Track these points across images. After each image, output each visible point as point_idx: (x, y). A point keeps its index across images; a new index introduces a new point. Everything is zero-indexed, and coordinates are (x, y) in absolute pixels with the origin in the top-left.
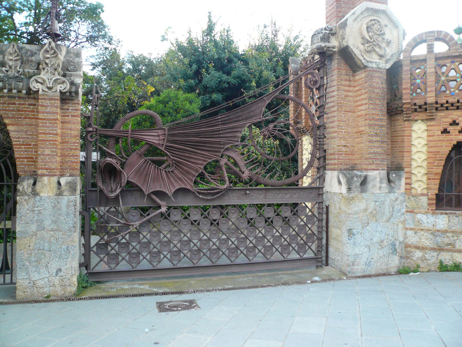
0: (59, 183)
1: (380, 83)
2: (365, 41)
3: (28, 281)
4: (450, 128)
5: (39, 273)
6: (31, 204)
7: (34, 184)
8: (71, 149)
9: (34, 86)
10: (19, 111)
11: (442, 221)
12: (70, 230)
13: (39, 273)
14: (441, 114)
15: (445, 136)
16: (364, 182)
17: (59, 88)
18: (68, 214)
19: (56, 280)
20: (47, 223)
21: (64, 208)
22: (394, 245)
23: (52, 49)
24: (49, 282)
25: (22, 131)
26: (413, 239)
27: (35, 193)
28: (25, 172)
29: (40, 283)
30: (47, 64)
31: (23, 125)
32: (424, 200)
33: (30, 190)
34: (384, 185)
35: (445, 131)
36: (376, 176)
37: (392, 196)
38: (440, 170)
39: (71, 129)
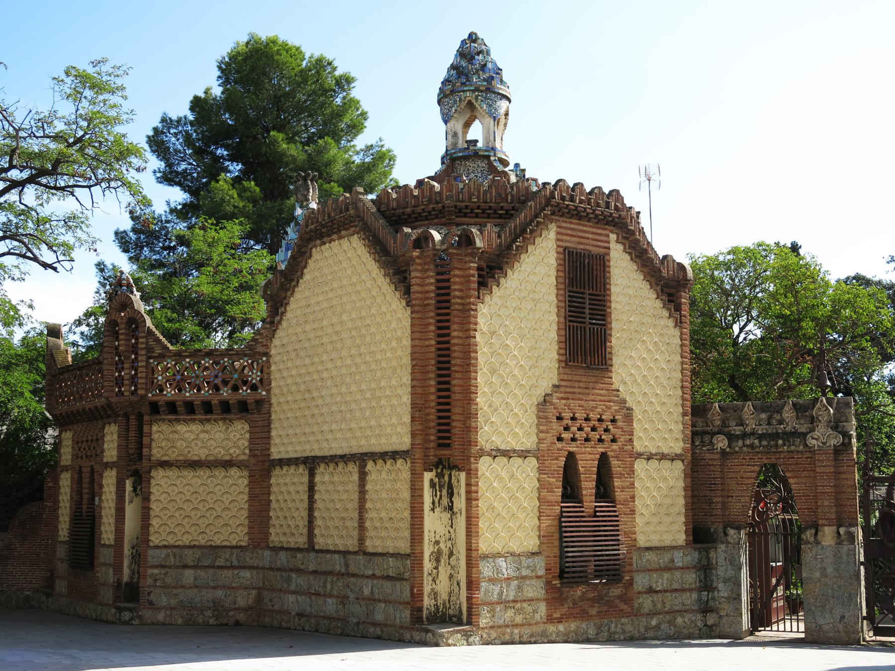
0: (838, 533)
3: (814, 625)
5: (825, 618)
6: (814, 552)
7: (816, 534)
8: (848, 499)
9: (811, 442)
10: (797, 464)
12: (851, 578)
13: (825, 618)
17: (833, 442)
18: (848, 563)
19: (840, 627)
20: (829, 570)
21: (845, 557)
23: (824, 406)
24: (834, 627)
25: (802, 483)
27: (818, 543)
28: (806, 522)
29: (826, 628)
30: (820, 421)
31: (801, 478)
33: (813, 539)
39: (847, 479)
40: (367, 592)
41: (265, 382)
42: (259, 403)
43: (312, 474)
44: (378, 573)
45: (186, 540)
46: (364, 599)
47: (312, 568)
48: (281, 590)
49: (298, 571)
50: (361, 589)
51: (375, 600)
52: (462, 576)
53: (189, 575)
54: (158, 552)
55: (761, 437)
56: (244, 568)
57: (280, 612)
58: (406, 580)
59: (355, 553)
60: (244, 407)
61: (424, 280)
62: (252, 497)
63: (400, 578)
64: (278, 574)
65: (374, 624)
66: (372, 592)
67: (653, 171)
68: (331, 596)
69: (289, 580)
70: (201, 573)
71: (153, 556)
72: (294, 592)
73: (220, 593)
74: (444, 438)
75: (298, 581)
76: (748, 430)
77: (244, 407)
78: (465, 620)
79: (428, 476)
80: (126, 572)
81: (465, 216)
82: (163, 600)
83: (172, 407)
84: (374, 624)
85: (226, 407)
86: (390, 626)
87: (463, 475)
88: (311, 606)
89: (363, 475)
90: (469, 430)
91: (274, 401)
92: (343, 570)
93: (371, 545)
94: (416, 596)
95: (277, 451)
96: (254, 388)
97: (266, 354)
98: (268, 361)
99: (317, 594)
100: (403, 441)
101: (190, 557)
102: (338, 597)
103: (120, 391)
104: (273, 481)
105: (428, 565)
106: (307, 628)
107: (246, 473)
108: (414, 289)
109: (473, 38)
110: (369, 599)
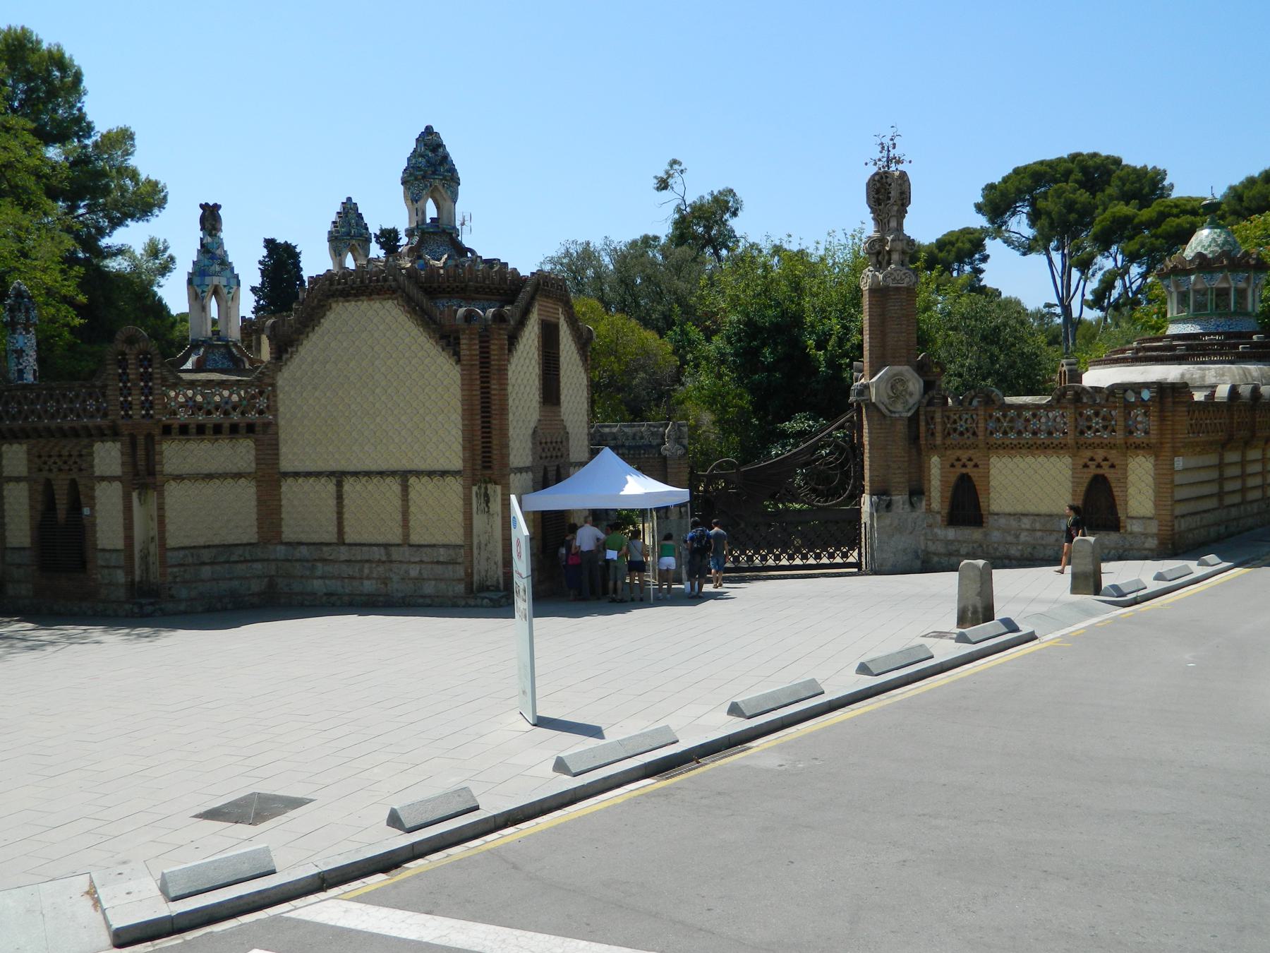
1: (901, 428)
2: (890, 398)
4: (956, 463)
11: (951, 533)
14: (949, 452)
15: (952, 470)
16: (889, 506)
22: (916, 552)
26: (932, 547)
27: (667, 518)
32: (939, 518)
34: (907, 506)
35: (953, 466)
36: (899, 499)
37: (914, 515)
38: (949, 494)
40: (414, 571)
41: (272, 408)
42: (267, 425)
43: (339, 485)
44: (425, 559)
45: (201, 541)
47: (343, 558)
49: (324, 561)
50: (407, 572)
52: (499, 557)
53: (206, 571)
54: (176, 553)
55: (630, 448)
56: (257, 561)
59: (398, 545)
60: (251, 428)
61: (469, 346)
62: (261, 502)
63: (453, 562)
64: (298, 565)
67: (467, 218)
68: (368, 578)
70: (218, 568)
71: (173, 557)
72: (321, 578)
73: (236, 583)
74: (487, 463)
75: (320, 569)
76: (619, 443)
77: (251, 428)
78: (502, 586)
79: (475, 489)
80: (137, 572)
81: (478, 293)
82: (184, 593)
83: (184, 430)
84: (422, 597)
85: (234, 429)
87: (499, 488)
89: (405, 489)
90: (505, 456)
91: (282, 422)
92: (384, 558)
93: (415, 538)
94: (470, 575)
95: (286, 465)
96: (261, 412)
97: (273, 385)
98: (274, 391)
100: (457, 464)
101: (206, 555)
103: (127, 414)
104: (284, 489)
105: (475, 551)
107: (253, 483)
108: (462, 353)
109: (429, 130)
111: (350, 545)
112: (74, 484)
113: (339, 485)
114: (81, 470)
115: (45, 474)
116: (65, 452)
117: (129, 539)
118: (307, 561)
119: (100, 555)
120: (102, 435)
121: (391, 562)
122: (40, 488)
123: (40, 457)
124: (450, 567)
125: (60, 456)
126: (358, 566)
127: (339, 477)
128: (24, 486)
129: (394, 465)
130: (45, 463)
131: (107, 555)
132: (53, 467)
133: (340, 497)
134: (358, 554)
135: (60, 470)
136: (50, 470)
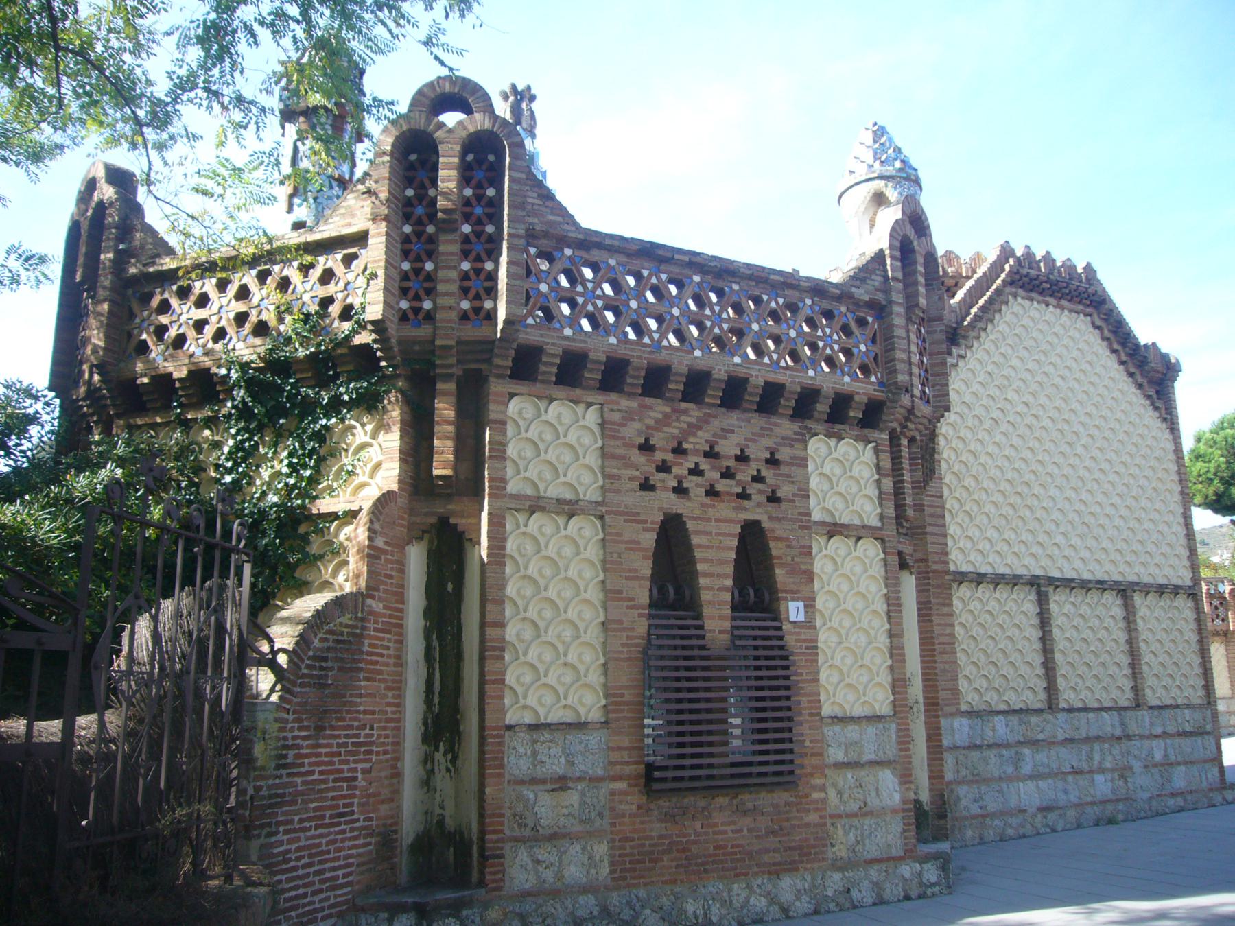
40: (1158, 756)
44: (1171, 729)
46: (1155, 766)
47: (1061, 736)
48: (1000, 778)
49: (1034, 743)
50: (1150, 753)
51: (1171, 764)
57: (1001, 814)
58: (1208, 733)
64: (992, 754)
65: (1173, 795)
66: (1166, 755)
68: (1102, 771)
69: (1017, 760)
84: (1173, 795)
86: (1196, 791)
88: (1066, 792)
92: (1118, 732)
99: (1076, 772)
102: (1113, 770)
106: (1059, 827)
110: (1163, 765)
111: (1070, 710)
112: (752, 542)
113: (1042, 600)
114: (773, 499)
115: (665, 501)
116: (729, 448)
117: (899, 683)
118: (1007, 746)
119: (831, 732)
120: (839, 413)
121: (1129, 737)
122: (649, 539)
123: (646, 447)
124: (1199, 740)
125: (711, 454)
126: (1085, 748)
127: (1041, 587)
128: (585, 530)
129: (1115, 574)
130: (664, 468)
131: (852, 732)
132: (691, 482)
133: (1044, 620)
134: (1085, 725)
135: (712, 492)
136: (680, 490)
